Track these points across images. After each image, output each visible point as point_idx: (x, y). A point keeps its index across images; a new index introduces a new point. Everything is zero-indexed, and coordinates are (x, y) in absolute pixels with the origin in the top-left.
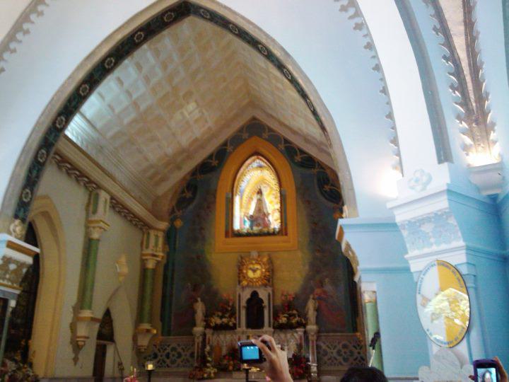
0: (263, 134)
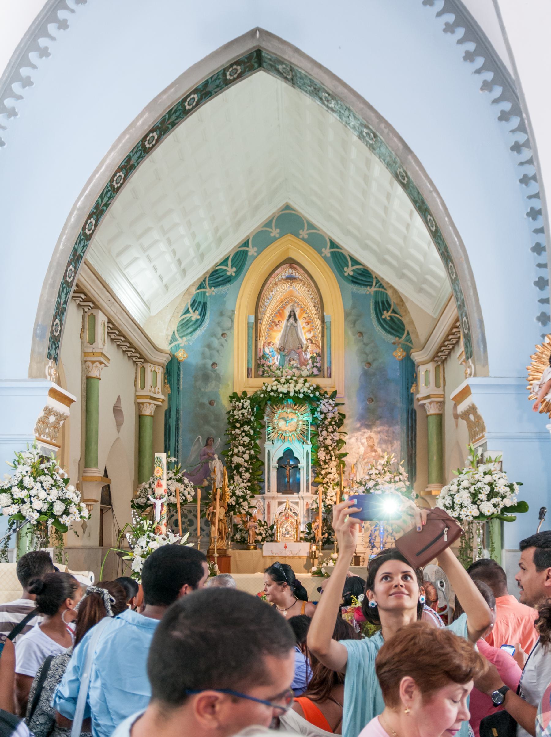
0: (301, 232)
